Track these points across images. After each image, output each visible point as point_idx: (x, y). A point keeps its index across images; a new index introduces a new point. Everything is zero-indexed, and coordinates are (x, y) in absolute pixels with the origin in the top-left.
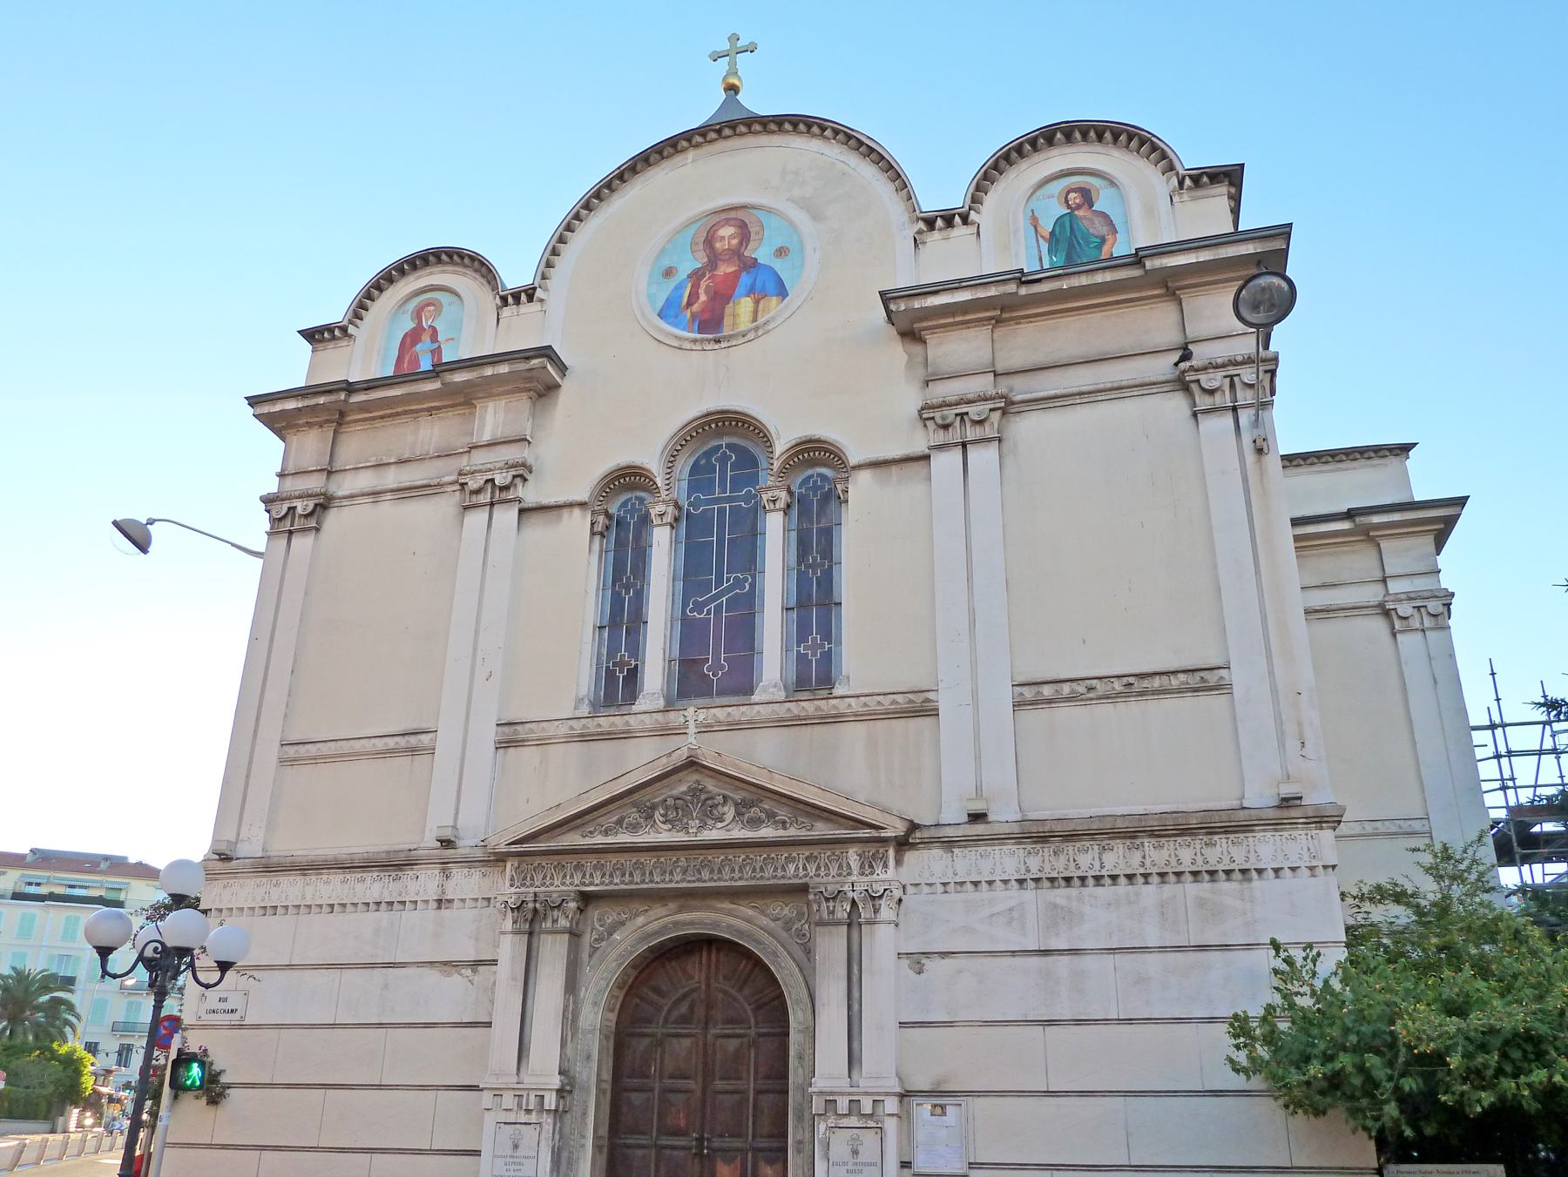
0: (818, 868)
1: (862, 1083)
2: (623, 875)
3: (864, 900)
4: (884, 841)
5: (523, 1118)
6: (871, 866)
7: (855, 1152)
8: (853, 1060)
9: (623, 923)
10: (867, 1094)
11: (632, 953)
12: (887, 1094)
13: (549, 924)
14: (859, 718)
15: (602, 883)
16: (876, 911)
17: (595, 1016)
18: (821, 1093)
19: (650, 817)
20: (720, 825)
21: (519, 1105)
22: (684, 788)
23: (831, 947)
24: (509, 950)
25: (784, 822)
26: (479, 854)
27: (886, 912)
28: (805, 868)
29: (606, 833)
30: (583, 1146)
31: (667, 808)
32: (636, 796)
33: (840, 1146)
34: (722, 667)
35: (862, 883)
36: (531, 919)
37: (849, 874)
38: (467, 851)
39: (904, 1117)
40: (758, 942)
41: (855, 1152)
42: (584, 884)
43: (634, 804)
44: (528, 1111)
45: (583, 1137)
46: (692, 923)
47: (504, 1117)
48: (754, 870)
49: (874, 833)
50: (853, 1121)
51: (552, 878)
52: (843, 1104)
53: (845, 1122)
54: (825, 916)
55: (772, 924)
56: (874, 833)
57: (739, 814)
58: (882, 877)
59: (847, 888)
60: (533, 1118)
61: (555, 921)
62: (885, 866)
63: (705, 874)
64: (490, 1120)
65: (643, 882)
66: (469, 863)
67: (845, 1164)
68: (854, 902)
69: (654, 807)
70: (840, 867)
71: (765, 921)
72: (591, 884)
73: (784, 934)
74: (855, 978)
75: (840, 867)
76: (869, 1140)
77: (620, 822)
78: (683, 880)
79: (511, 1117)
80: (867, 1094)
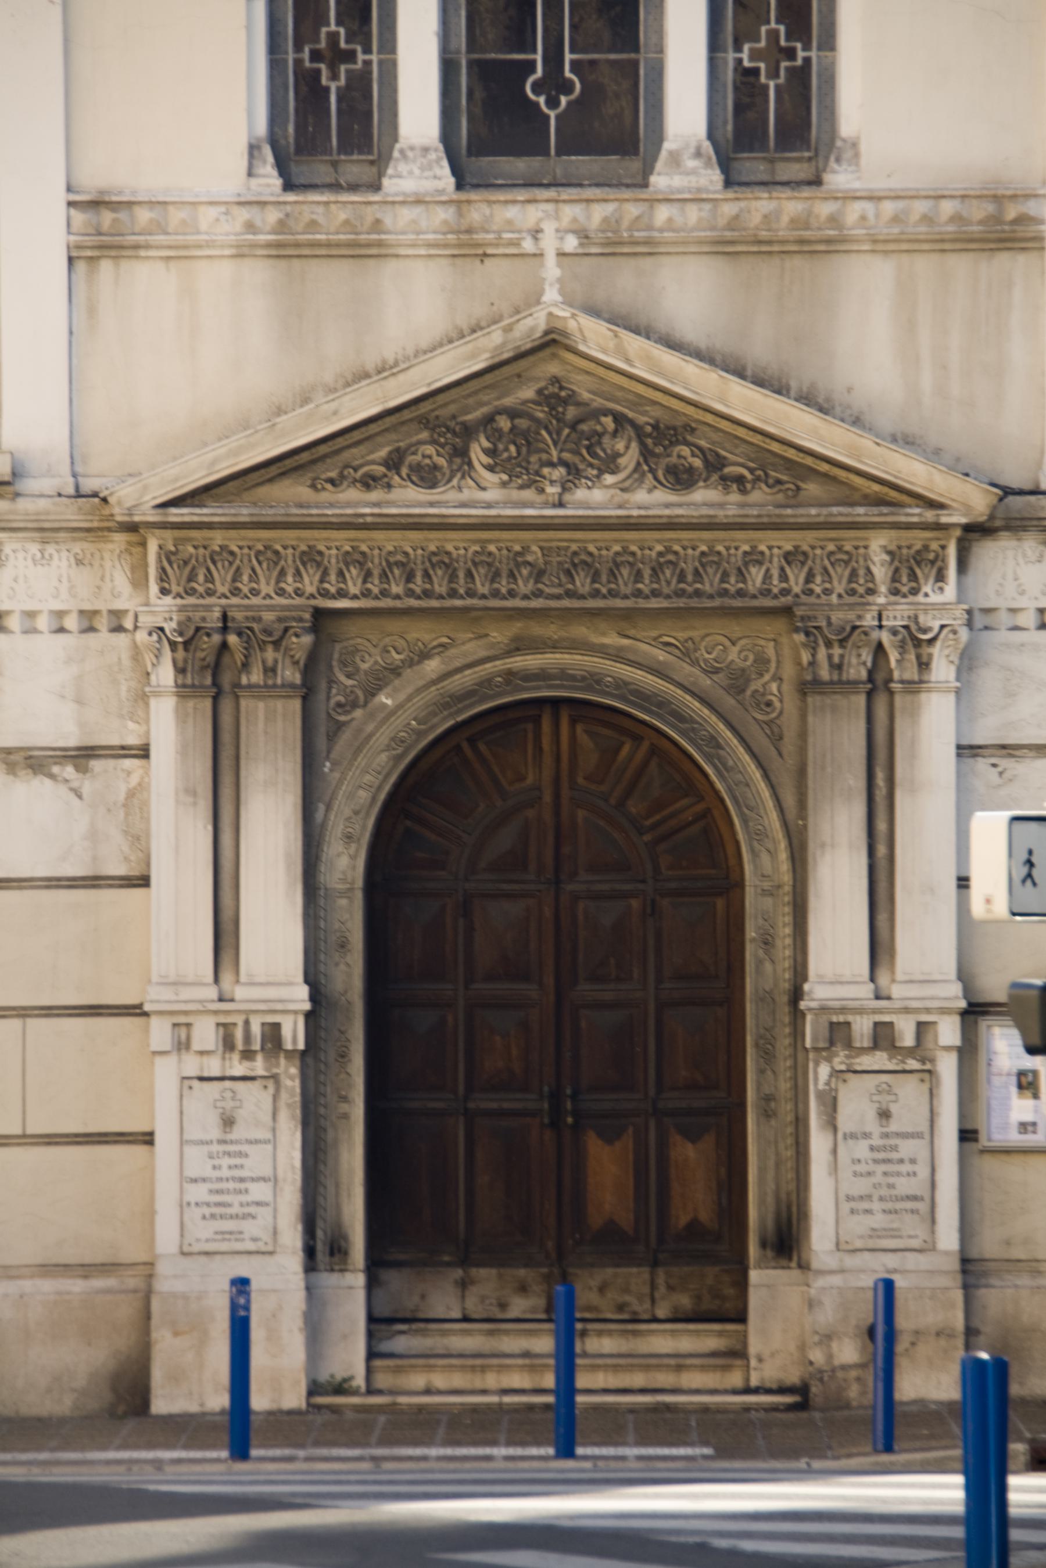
0: (810, 578)
1: (896, 991)
2: (410, 578)
3: (902, 647)
4: (938, 527)
5: (239, 1068)
6: (913, 577)
7: (885, 1115)
8: (880, 949)
9: (396, 671)
10: (907, 1010)
11: (420, 734)
12: (943, 1011)
13: (256, 676)
14: (881, 245)
15: (366, 594)
16: (924, 665)
17: (346, 864)
18: (824, 1009)
19: (461, 453)
20: (609, 479)
21: (228, 1044)
22: (528, 393)
23: (839, 737)
24: (167, 725)
25: (740, 480)
26: (71, 514)
27: (943, 669)
28: (784, 577)
29: (368, 482)
30: (346, 1116)
31: (496, 435)
32: (424, 408)
33: (856, 1105)
34: (567, 87)
35: (898, 615)
36: (212, 666)
37: (871, 592)
38: (42, 504)
39: (969, 1051)
40: (679, 717)
41: (885, 1115)
42: (325, 594)
43: (424, 422)
44: (248, 1055)
45: (345, 1099)
46: (542, 676)
47: (192, 1065)
48: (682, 578)
49: (930, 515)
50: (880, 1060)
51: (254, 576)
52: (862, 1027)
53: (866, 1062)
54: (825, 674)
55: (706, 682)
56: (930, 515)
57: (646, 454)
58: (935, 598)
59: (869, 620)
60: (259, 1066)
61: (270, 670)
62: (940, 577)
63: (582, 583)
64: (166, 1074)
65: (453, 594)
66: (45, 532)
67: (866, 1136)
68: (880, 649)
69: (468, 432)
70: (853, 575)
71: (686, 671)
72: (342, 594)
73: (731, 701)
74: (881, 793)
75: (853, 575)
76: (909, 1094)
77: (394, 463)
78: (538, 594)
79: (214, 1067)
80: (907, 1010)
